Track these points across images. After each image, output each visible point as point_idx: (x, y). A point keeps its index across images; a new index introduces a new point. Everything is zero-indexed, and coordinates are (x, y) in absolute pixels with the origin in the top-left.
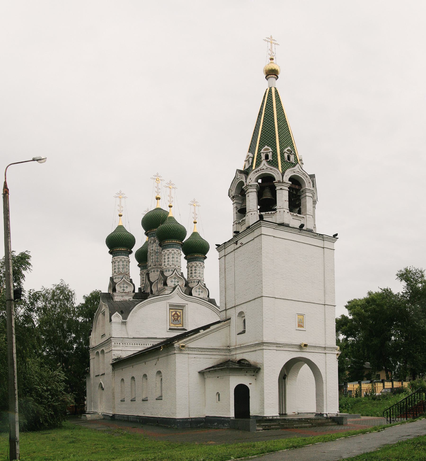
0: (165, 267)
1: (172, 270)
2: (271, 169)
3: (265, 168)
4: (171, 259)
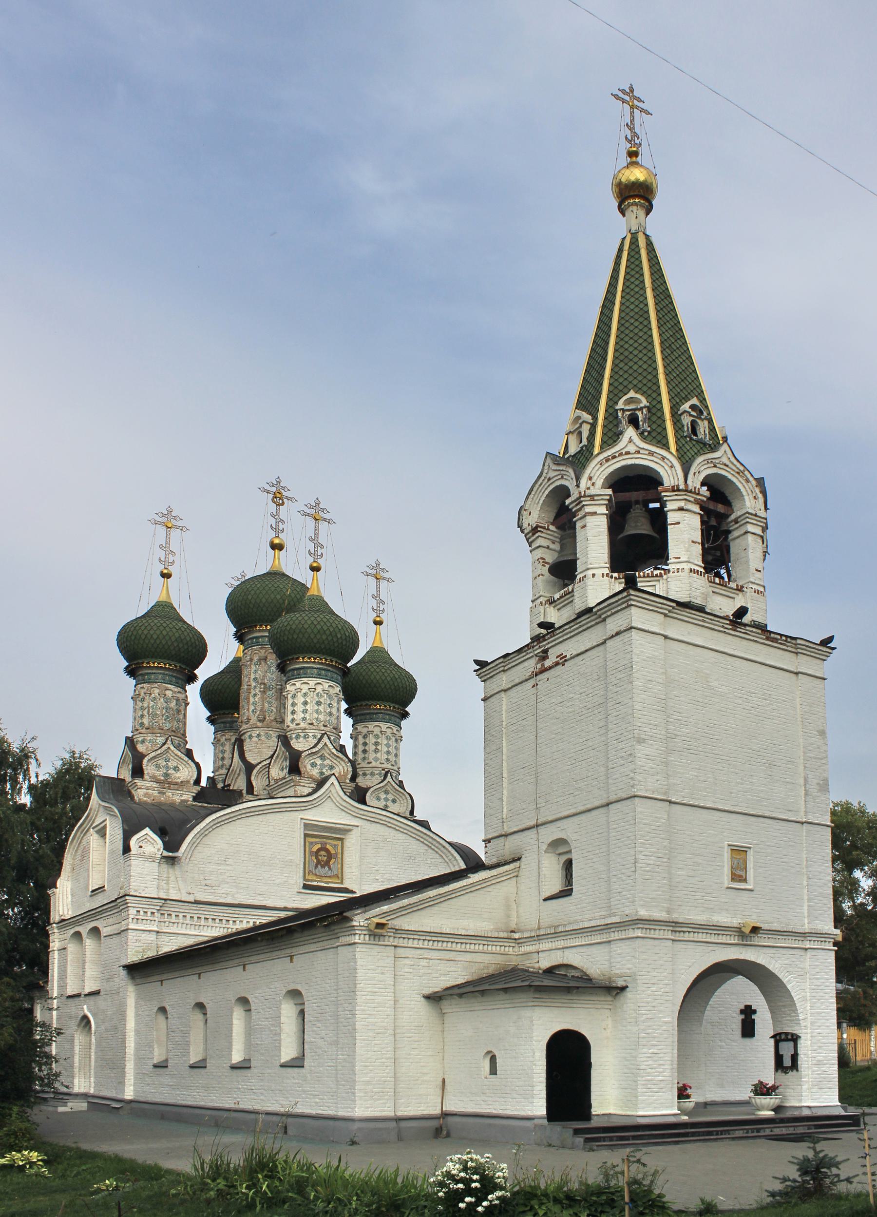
0: (292, 726)
2: (651, 453)
3: (633, 449)
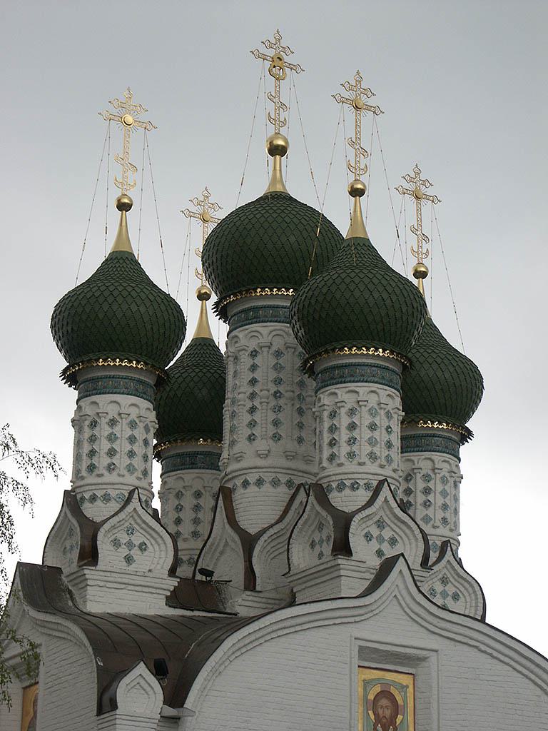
1: (367, 486)
4: (364, 434)
